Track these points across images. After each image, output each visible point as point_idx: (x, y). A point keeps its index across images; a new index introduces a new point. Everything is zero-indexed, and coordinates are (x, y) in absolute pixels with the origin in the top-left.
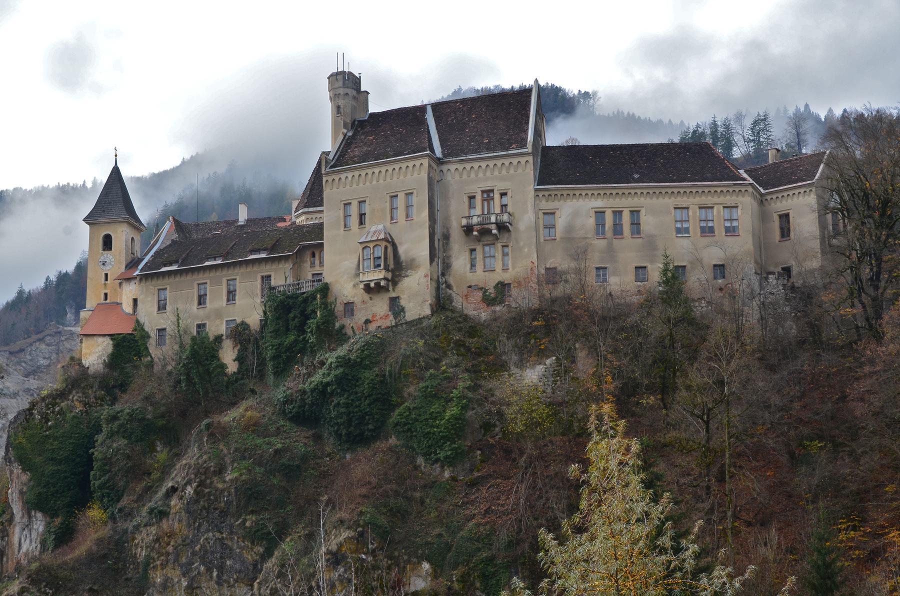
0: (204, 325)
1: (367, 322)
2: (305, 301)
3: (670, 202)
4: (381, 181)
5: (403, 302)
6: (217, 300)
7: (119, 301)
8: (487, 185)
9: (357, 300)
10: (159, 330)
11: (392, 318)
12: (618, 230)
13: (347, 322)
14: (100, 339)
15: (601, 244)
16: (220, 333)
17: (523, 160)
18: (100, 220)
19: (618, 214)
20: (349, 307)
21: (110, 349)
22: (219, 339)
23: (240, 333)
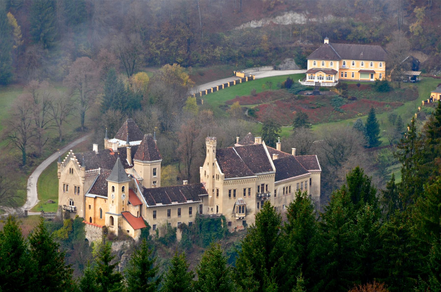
0: (170, 224)
1: (236, 228)
2: (218, 221)
3: (296, 182)
4: (241, 184)
5: (247, 222)
6: (174, 215)
7: (128, 211)
8: (262, 183)
9: (233, 221)
10: (154, 225)
11: (243, 227)
12: (287, 193)
13: (229, 228)
14: (138, 230)
15: (284, 197)
16: (176, 226)
17: (273, 175)
18: (123, 182)
19: (287, 187)
20: (230, 223)
21: (140, 233)
22: (175, 229)
23: (182, 227)
